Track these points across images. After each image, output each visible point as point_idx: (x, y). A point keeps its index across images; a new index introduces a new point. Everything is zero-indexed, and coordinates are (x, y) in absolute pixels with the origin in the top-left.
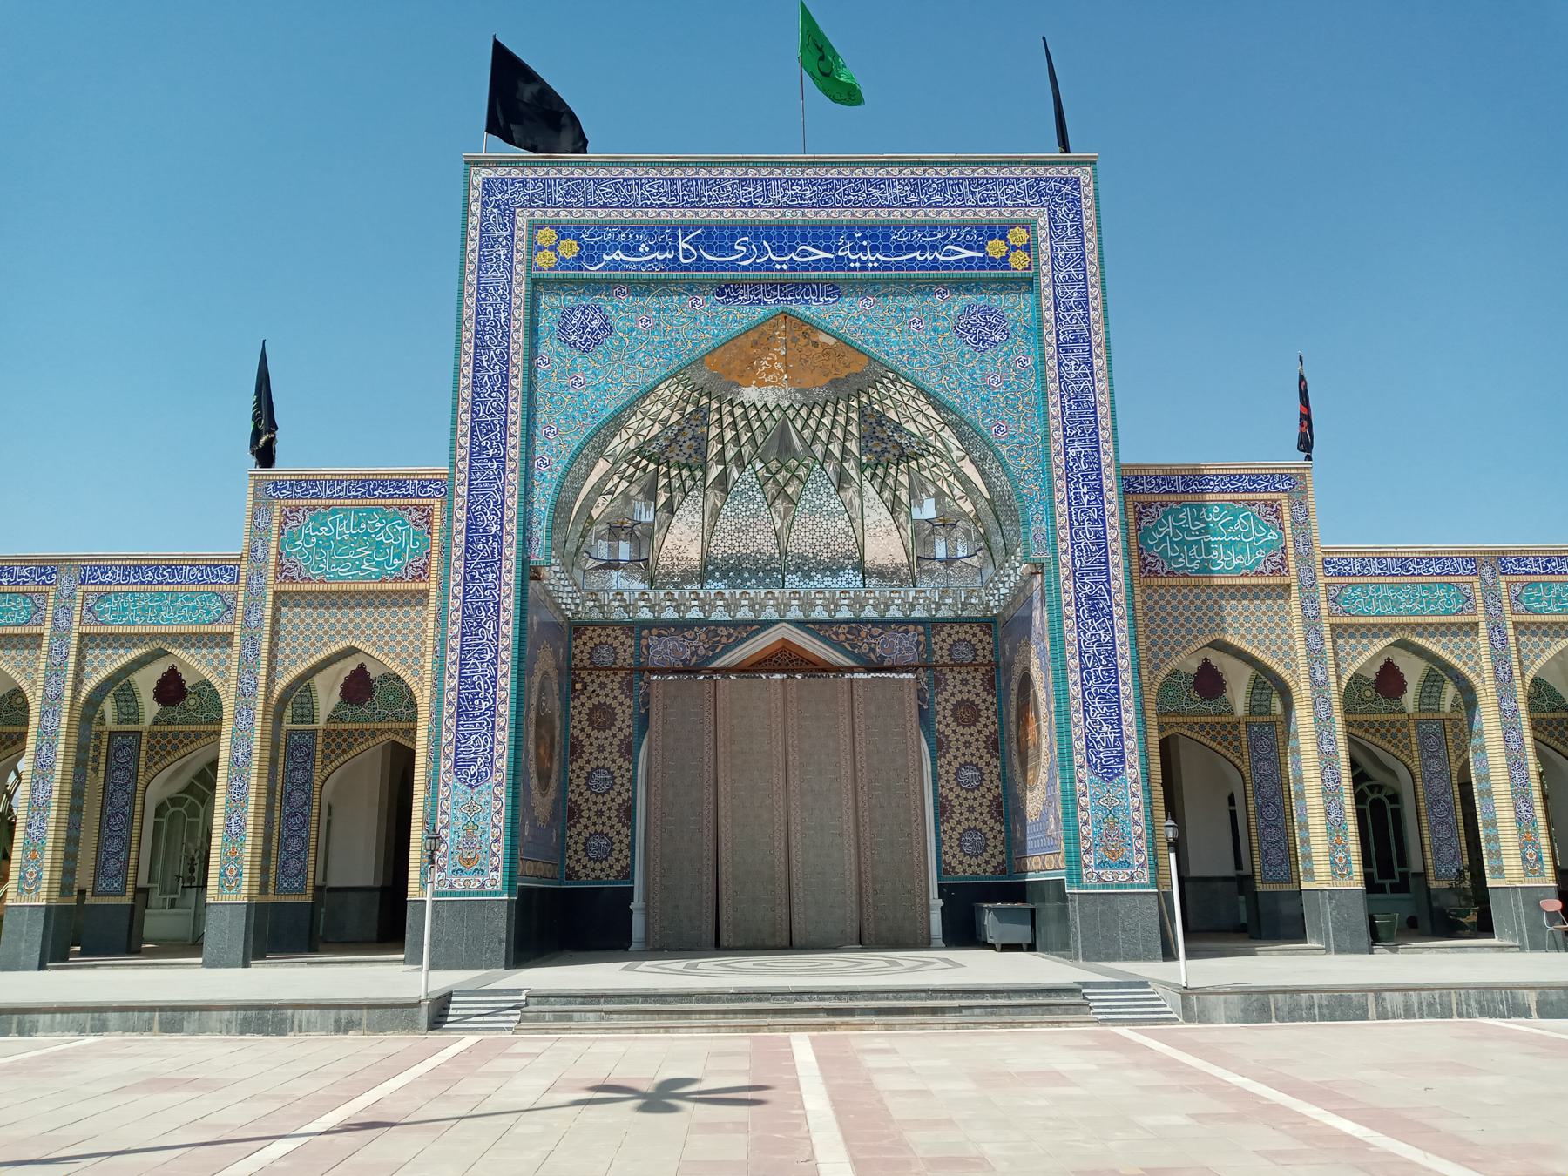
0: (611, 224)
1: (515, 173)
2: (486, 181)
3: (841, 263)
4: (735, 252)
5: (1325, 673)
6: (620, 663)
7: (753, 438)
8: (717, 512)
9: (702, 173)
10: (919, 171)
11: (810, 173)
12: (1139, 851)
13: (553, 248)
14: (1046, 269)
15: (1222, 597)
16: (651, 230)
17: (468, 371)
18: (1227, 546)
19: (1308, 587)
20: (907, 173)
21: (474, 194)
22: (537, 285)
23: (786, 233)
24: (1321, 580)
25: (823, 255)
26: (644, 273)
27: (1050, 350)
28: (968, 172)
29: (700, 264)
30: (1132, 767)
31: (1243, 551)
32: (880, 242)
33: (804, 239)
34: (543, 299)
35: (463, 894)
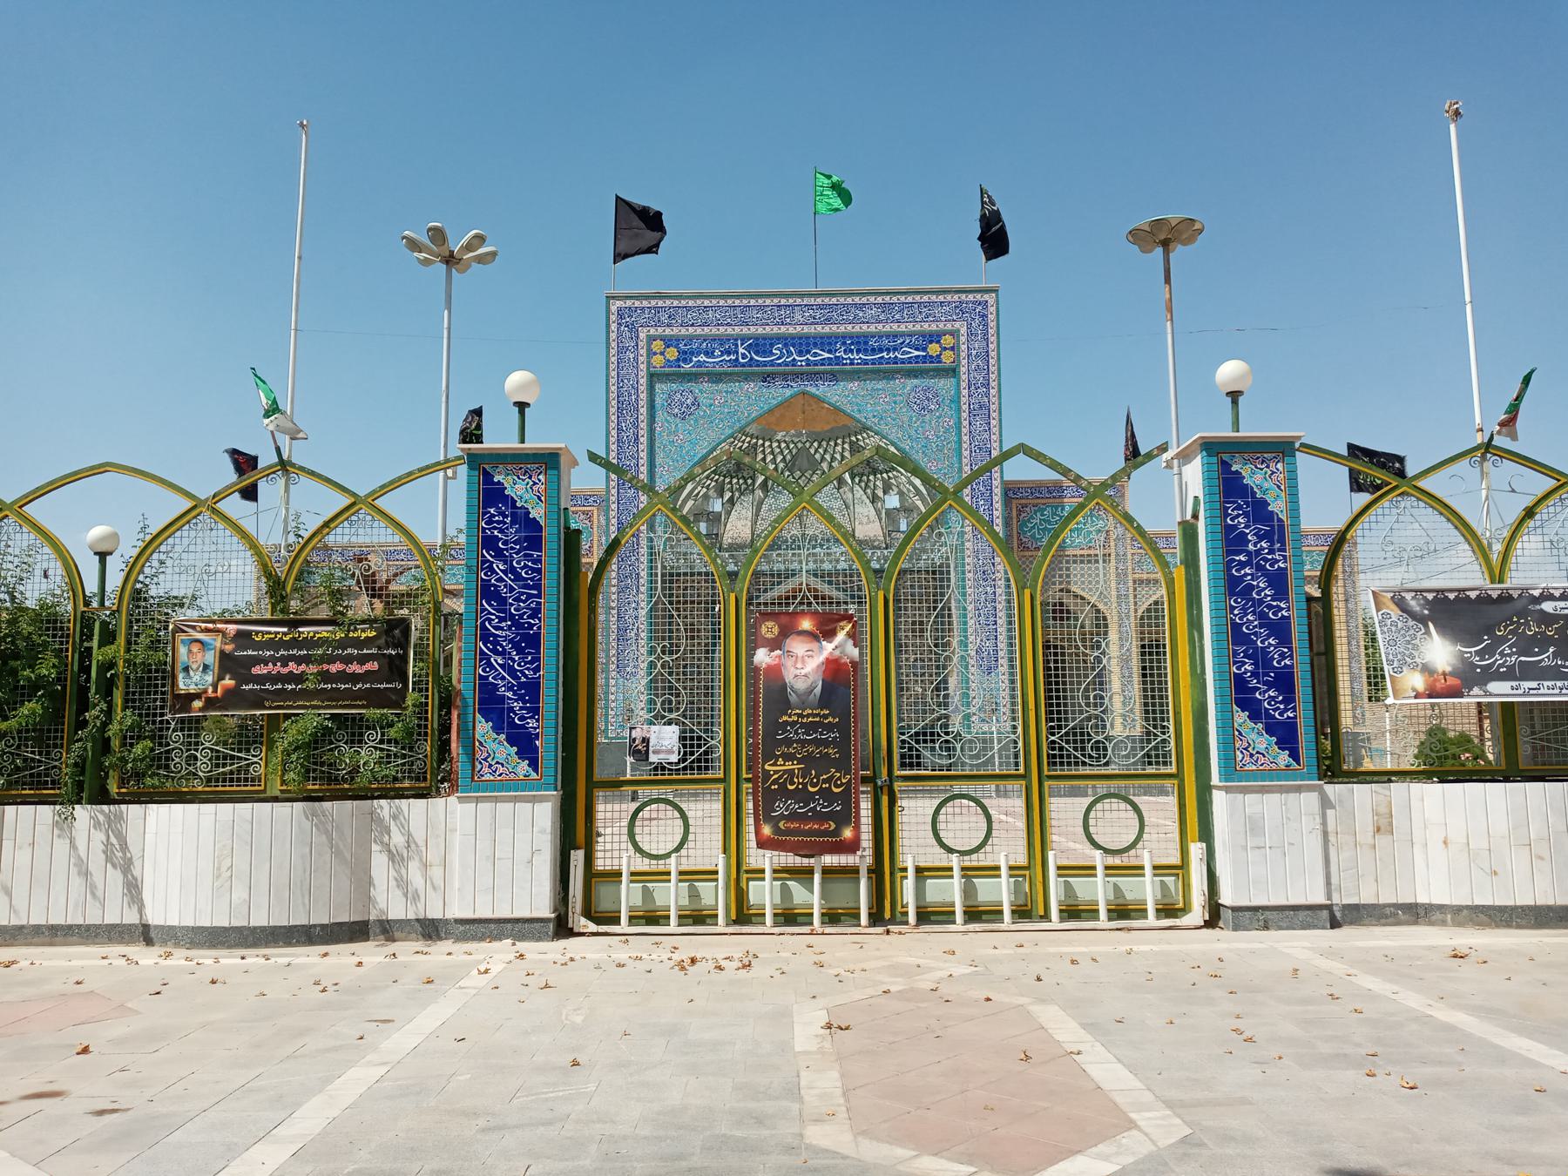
0: (698, 337)
1: (637, 304)
2: (620, 309)
3: (838, 361)
7: (784, 459)
8: (761, 503)
9: (753, 302)
10: (887, 299)
11: (819, 301)
13: (662, 354)
14: (964, 362)
16: (722, 340)
17: (614, 433)
20: (880, 300)
21: (613, 318)
22: (653, 377)
23: (803, 341)
25: (827, 355)
26: (718, 368)
27: (965, 415)
28: (918, 298)
32: (862, 347)
33: (815, 345)
34: (658, 386)
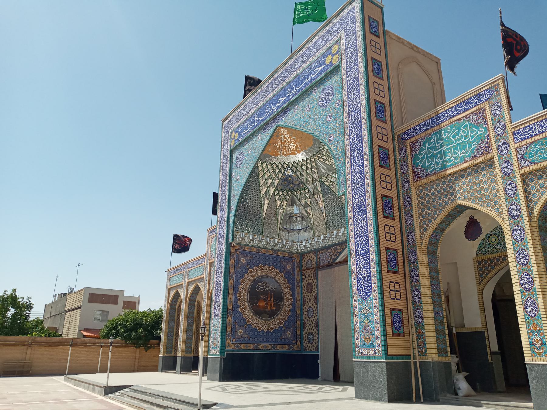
4: (265, 112)
5: (519, 209)
6: (313, 266)
12: (378, 338)
15: (456, 179)
18: (455, 148)
19: (504, 154)
24: (513, 147)
25: (284, 99)
29: (260, 122)
30: (375, 291)
31: (464, 148)
35: (213, 355)
